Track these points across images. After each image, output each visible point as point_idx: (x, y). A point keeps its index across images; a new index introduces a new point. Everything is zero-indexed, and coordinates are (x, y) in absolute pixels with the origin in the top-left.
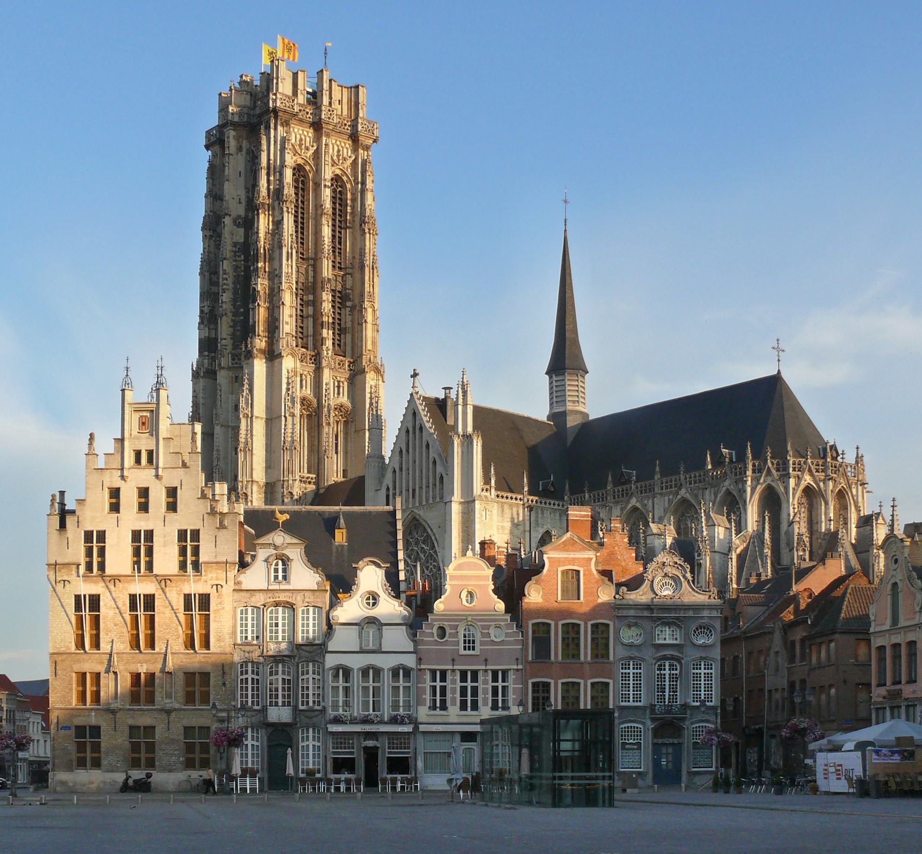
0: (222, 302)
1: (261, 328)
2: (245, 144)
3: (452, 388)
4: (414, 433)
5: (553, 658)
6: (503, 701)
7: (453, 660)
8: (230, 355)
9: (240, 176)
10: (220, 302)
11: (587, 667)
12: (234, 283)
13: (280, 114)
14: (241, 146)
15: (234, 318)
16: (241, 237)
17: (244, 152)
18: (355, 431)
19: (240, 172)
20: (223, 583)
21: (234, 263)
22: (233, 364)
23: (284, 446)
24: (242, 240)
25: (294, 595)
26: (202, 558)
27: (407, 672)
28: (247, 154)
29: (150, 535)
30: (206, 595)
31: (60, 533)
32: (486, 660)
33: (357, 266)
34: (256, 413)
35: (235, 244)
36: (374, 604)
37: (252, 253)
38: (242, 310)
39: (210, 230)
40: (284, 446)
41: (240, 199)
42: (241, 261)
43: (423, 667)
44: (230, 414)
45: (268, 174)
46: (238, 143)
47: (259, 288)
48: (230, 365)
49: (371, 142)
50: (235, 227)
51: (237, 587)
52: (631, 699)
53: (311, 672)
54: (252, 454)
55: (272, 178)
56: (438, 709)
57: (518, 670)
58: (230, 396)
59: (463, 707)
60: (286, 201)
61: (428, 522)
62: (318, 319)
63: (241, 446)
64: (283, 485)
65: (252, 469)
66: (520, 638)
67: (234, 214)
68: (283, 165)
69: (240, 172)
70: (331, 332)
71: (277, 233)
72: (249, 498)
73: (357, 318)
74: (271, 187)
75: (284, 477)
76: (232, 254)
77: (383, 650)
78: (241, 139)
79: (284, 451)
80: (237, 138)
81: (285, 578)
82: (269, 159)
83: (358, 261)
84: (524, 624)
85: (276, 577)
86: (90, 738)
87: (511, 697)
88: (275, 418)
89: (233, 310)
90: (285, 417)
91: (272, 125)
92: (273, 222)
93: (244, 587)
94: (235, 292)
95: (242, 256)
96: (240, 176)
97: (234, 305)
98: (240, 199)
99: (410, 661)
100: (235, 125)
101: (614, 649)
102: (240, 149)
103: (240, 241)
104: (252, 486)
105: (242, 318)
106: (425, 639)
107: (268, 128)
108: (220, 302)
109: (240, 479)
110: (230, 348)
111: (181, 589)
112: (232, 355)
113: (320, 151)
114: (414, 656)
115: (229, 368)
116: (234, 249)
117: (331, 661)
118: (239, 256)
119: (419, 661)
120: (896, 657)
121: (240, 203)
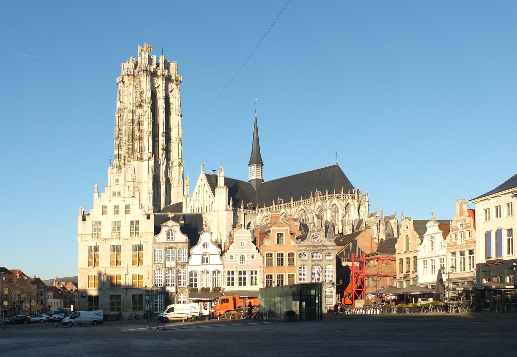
3: (215, 171)
4: (201, 187)
5: (273, 265)
6: (255, 282)
7: (237, 267)
10: (123, 140)
11: (286, 268)
12: (128, 134)
15: (128, 146)
18: (174, 187)
20: (149, 240)
24: (131, 118)
25: (176, 244)
26: (140, 231)
27: (219, 272)
29: (119, 222)
30: (135, 245)
31: (83, 222)
32: (249, 267)
35: (129, 120)
36: (206, 247)
37: (136, 123)
42: (131, 126)
43: (225, 270)
49: (180, 83)
51: (154, 242)
52: (303, 280)
53: (182, 273)
56: (231, 286)
57: (261, 270)
59: (240, 284)
61: (207, 219)
66: (262, 259)
69: (131, 93)
77: (210, 264)
80: (129, 80)
81: (172, 238)
84: (263, 253)
85: (169, 238)
86: (94, 300)
87: (258, 281)
89: (128, 144)
93: (157, 242)
95: (132, 124)
96: (131, 94)
99: (220, 268)
101: (296, 262)
106: (226, 260)
108: (123, 140)
111: (132, 243)
114: (222, 266)
117: (190, 269)
118: (130, 124)
119: (224, 267)
120: (408, 263)
121: (131, 104)
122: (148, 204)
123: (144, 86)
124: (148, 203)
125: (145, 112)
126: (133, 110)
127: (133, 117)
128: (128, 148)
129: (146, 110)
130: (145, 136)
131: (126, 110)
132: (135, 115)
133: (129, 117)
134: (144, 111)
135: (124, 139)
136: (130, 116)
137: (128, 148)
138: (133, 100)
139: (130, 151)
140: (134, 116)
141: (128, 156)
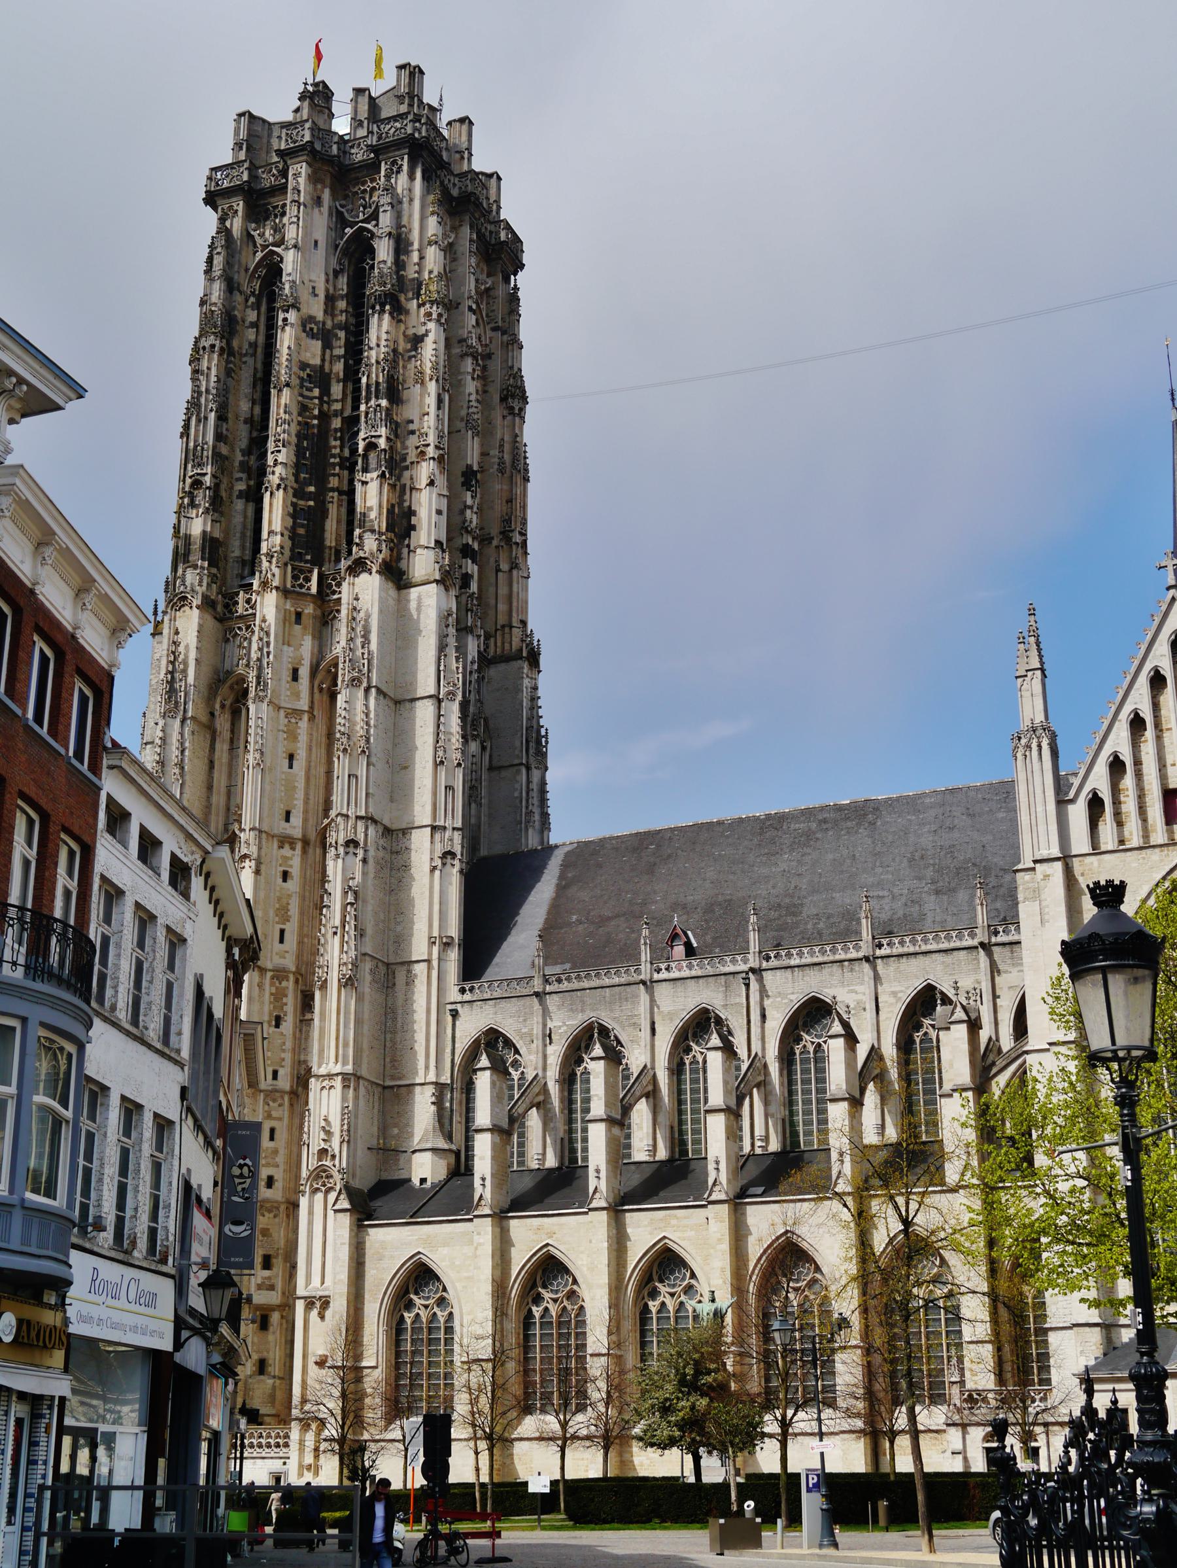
0: (276, 463)
2: (326, 195)
8: (289, 567)
12: (298, 435)
14: (319, 198)
16: (314, 356)
17: (325, 209)
18: (491, 768)
21: (300, 399)
22: (293, 586)
24: (317, 361)
28: (330, 214)
35: (303, 366)
38: (312, 489)
41: (314, 288)
44: (283, 683)
46: (315, 189)
48: (289, 585)
50: (304, 335)
58: (285, 648)
69: (316, 242)
71: (414, 356)
73: (492, 560)
76: (298, 381)
78: (319, 186)
80: (313, 179)
89: (295, 485)
94: (299, 452)
95: (316, 392)
97: (296, 475)
98: (314, 288)
103: (312, 362)
105: (312, 503)
112: (293, 569)
116: (301, 374)
118: (310, 390)
122: (442, 823)
123: (410, 216)
124: (434, 818)
125: (417, 341)
127: (323, 360)
128: (295, 510)
129: (422, 330)
130: (412, 456)
131: (292, 316)
132: (328, 351)
133: (303, 353)
134: (410, 332)
135: (281, 458)
136: (313, 352)
137: (291, 510)
138: (327, 281)
139: (302, 526)
140: (327, 357)
141: (292, 550)
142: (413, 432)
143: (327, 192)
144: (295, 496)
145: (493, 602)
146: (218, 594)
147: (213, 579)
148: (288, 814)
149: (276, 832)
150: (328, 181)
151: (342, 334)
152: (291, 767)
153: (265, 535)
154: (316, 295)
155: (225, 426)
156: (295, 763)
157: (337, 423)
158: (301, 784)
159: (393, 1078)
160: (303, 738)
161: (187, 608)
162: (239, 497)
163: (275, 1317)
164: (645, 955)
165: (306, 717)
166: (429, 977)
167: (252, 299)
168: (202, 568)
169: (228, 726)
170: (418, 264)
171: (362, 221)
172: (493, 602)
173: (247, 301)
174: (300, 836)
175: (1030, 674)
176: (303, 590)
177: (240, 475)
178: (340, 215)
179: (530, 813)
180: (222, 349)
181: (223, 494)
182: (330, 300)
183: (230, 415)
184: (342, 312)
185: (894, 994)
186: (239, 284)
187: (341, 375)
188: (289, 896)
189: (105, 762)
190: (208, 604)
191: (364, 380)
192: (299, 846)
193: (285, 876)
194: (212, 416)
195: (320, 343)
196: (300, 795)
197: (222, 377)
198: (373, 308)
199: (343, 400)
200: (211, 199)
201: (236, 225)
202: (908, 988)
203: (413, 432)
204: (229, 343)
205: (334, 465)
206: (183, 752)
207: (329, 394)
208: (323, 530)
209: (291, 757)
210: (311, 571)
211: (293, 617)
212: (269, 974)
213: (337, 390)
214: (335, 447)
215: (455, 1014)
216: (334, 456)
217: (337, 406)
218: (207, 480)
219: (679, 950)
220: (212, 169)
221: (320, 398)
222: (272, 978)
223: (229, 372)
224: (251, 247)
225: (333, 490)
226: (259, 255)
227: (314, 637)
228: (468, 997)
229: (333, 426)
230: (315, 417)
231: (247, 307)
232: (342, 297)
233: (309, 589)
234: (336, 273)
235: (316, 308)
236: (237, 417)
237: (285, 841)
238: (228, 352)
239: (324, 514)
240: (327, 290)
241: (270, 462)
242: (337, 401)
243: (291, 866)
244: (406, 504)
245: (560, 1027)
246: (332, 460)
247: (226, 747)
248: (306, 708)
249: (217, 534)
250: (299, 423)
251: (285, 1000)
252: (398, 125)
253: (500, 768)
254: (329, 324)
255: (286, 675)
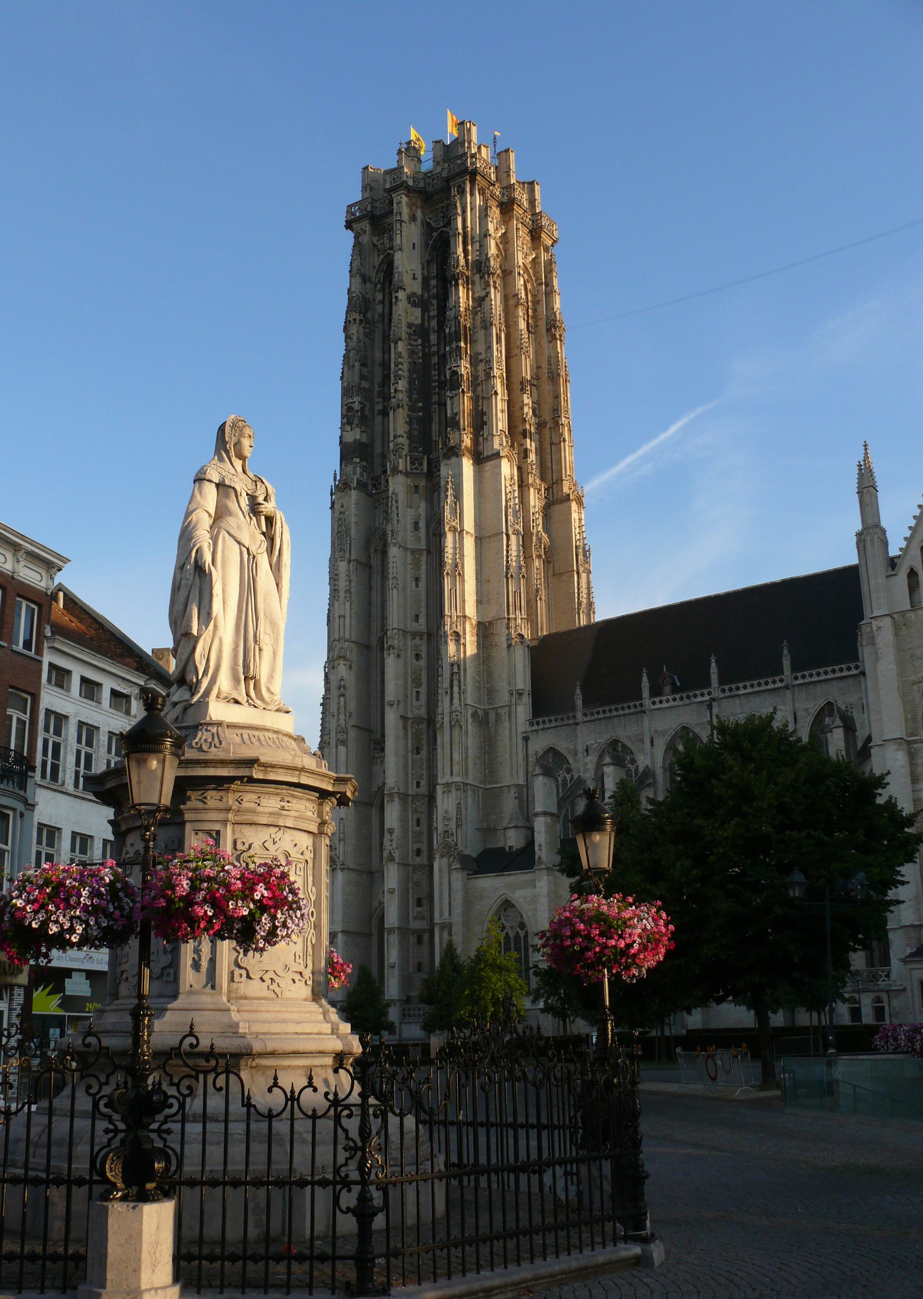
1: (465, 420)
2: (419, 214)
8: (408, 458)
9: (414, 248)
12: (409, 371)
13: (478, 178)
14: (414, 216)
16: (417, 317)
17: (419, 222)
18: (554, 575)
19: (414, 244)
21: (409, 347)
23: (507, 573)
28: (422, 225)
33: (545, 377)
34: (466, 528)
35: (410, 325)
38: (421, 404)
39: (360, 313)
40: (507, 573)
41: (414, 274)
42: (417, 346)
44: (409, 532)
45: (465, 244)
47: (463, 371)
48: (409, 469)
50: (409, 305)
54: (463, 581)
55: (470, 248)
58: (409, 510)
60: (493, 274)
62: (516, 427)
63: (448, 568)
64: (508, 624)
65: (464, 601)
67: (409, 290)
68: (485, 235)
69: (414, 244)
70: (533, 444)
71: (480, 311)
72: (462, 641)
73: (548, 437)
74: (470, 258)
75: (508, 614)
76: (407, 336)
78: (414, 208)
79: (507, 579)
80: (410, 205)
82: (464, 227)
83: (546, 371)
88: (490, 537)
89: (409, 404)
90: (508, 535)
91: (468, 189)
92: (473, 298)
94: (411, 382)
95: (420, 341)
96: (414, 248)
97: (410, 397)
98: (414, 274)
100: (409, 190)
102: (413, 218)
103: (416, 322)
104: (464, 623)
105: (421, 414)
107: (462, 192)
109: (447, 612)
110: (406, 448)
113: (509, 235)
115: (407, 474)
116: (409, 331)
118: (416, 340)
121: (414, 278)
126: (422, 296)
128: (410, 420)
132: (426, 314)
136: (415, 316)
138: (423, 268)
141: (410, 446)
142: (481, 361)
143: (419, 211)
144: (409, 410)
145: (549, 465)
146: (367, 479)
147: (363, 467)
148: (417, 616)
149: (409, 629)
150: (419, 204)
151: (435, 302)
152: (417, 586)
153: (391, 438)
154: (416, 279)
155: (366, 370)
156: (420, 584)
157: (435, 360)
158: (423, 597)
159: (490, 783)
160: (424, 567)
161: (347, 490)
162: (378, 414)
163: (426, 937)
164: (646, 693)
165: (425, 553)
166: (510, 717)
167: (379, 286)
168: (356, 463)
169: (379, 563)
170: (479, 250)
171: (442, 227)
172: (549, 465)
173: (376, 287)
174: (425, 631)
175: (864, 490)
176: (419, 471)
177: (377, 400)
178: (428, 224)
179: (580, 604)
180: (360, 320)
181: (367, 413)
182: (426, 281)
183: (369, 363)
184: (434, 287)
185: (807, 709)
186: (369, 277)
187: (436, 327)
188: (421, 670)
189: (46, 645)
190: (361, 486)
191: (447, 331)
192: (425, 636)
193: (418, 657)
194: (357, 364)
195: (420, 309)
196: (423, 604)
197: (361, 338)
198: (451, 283)
199: (438, 344)
200: (349, 225)
201: (365, 239)
202: (815, 705)
203: (481, 361)
204: (364, 316)
205: (435, 387)
206: (350, 582)
207: (429, 341)
208: (430, 430)
209: (417, 580)
210: (422, 459)
211: (413, 489)
212: (410, 722)
213: (433, 338)
214: (435, 375)
215: (526, 739)
216: (434, 381)
217: (434, 349)
218: (356, 406)
219: (667, 689)
220: (348, 206)
221: (423, 345)
222: (413, 723)
223: (366, 335)
224: (376, 253)
225: (435, 403)
226: (382, 257)
227: (427, 501)
228: (535, 727)
229: (433, 362)
230: (420, 358)
231: (376, 291)
232: (433, 278)
233: (422, 470)
234: (429, 262)
235: (416, 287)
236: (374, 362)
237: (415, 634)
238: (365, 322)
239: (430, 420)
240: (423, 274)
241: (392, 391)
242: (434, 345)
243: (421, 651)
244: (480, 408)
245: (593, 744)
246: (433, 384)
247: (379, 576)
248: (425, 547)
249: (364, 440)
250: (410, 363)
251: (422, 737)
252: (459, 162)
253: (561, 574)
254: (426, 295)
255: (410, 527)
